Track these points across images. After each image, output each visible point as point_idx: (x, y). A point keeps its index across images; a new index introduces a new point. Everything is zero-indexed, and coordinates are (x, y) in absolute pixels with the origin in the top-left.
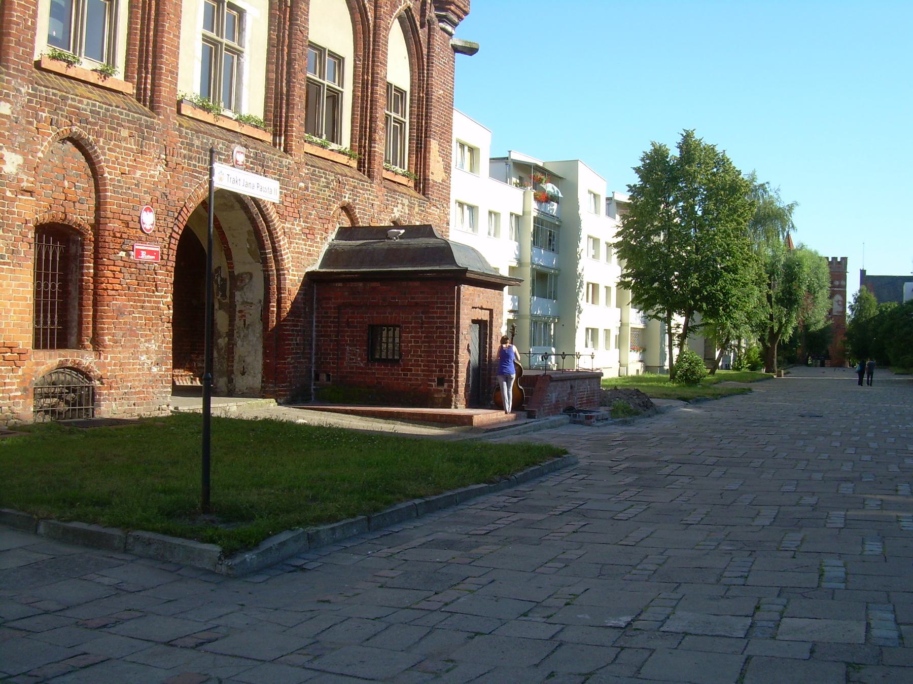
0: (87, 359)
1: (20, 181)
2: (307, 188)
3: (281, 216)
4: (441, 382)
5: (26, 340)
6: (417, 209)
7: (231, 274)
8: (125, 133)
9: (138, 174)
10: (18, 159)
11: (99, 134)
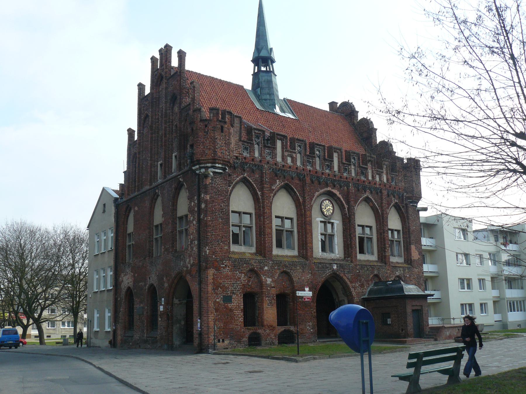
0: (292, 328)
1: (271, 285)
2: (359, 272)
3: (351, 282)
4: (402, 330)
5: (275, 324)
6: (407, 271)
7: (339, 300)
8: (298, 268)
9: (303, 278)
10: (271, 280)
11: (291, 270)
